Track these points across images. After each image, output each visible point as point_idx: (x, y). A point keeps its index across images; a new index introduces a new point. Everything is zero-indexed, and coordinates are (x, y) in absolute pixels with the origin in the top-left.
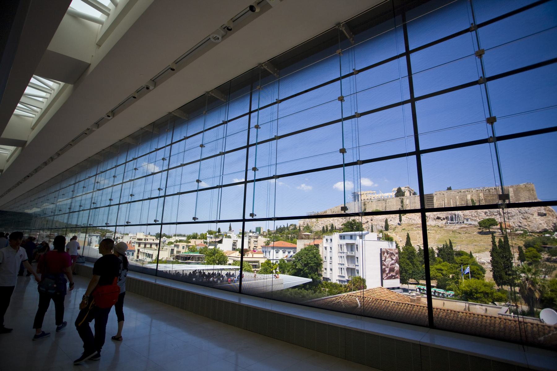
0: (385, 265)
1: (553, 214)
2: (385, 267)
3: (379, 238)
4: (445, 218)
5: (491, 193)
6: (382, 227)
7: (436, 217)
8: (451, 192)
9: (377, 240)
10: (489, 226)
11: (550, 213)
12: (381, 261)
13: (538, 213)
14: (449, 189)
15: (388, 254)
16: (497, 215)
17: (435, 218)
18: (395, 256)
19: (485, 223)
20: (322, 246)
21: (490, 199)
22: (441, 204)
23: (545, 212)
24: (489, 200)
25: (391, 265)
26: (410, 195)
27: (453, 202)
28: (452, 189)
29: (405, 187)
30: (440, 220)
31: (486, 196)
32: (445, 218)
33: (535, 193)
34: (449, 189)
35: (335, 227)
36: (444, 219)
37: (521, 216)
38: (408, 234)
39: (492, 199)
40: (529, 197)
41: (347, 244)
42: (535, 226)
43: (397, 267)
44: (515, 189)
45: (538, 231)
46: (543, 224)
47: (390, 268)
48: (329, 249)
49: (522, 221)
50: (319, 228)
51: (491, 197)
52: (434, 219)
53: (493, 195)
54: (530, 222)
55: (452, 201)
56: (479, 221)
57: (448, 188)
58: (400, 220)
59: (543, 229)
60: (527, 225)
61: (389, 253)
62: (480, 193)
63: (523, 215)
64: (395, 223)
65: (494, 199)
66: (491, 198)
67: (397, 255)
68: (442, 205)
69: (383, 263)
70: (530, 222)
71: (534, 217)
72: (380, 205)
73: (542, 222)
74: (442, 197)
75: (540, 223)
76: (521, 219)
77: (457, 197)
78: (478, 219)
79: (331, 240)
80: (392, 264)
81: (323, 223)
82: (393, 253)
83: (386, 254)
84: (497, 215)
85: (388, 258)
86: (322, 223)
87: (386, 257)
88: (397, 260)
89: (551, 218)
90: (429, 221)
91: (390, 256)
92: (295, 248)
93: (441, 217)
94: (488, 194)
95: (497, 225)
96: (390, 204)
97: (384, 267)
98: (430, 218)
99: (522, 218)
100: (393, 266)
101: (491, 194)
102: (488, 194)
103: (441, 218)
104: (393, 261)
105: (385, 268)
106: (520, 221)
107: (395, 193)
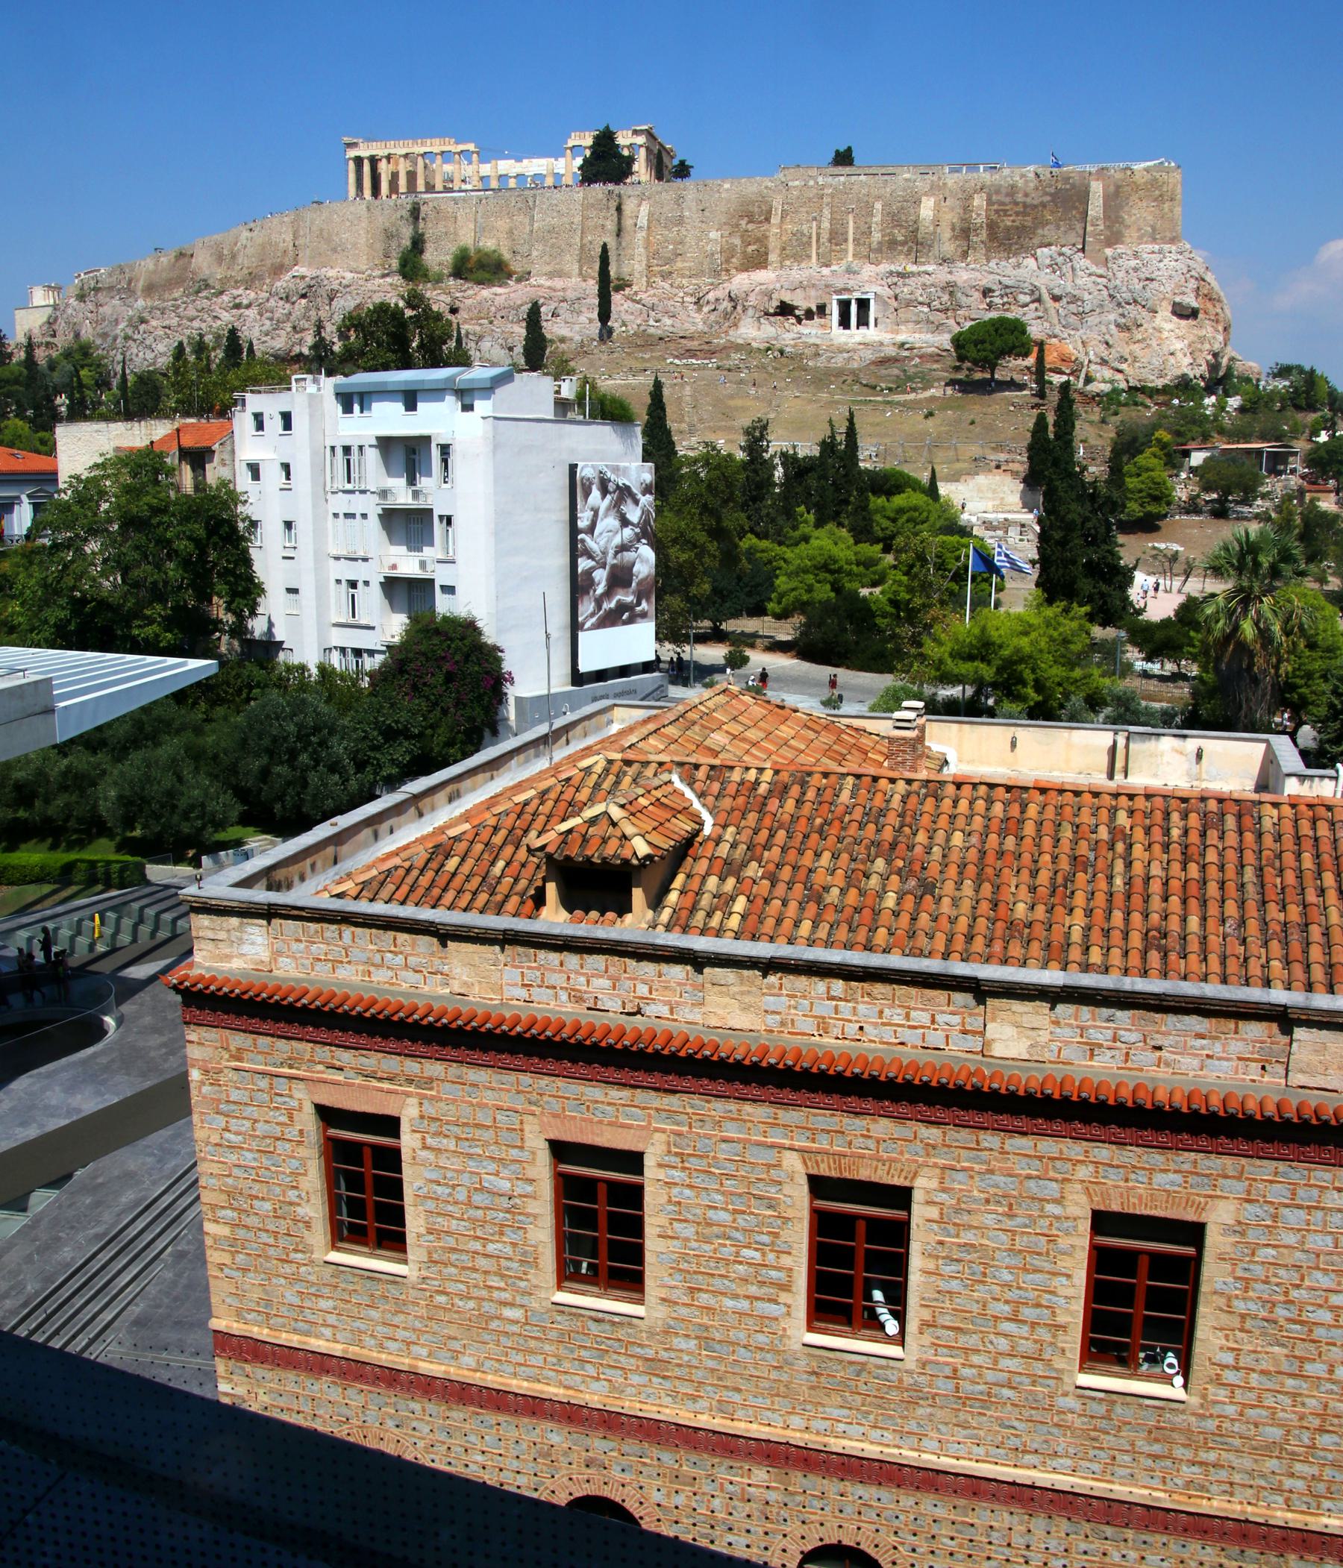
0: (589, 555)
1: (1219, 311)
2: (590, 563)
3: (562, 406)
4: (814, 309)
5: (1020, 198)
6: (511, 349)
7: (775, 303)
8: (854, 178)
9: (552, 417)
10: (998, 358)
11: (1209, 305)
12: (574, 530)
13: (1175, 304)
14: (844, 158)
15: (604, 491)
16: (1026, 305)
17: (772, 311)
18: (636, 502)
19: (983, 342)
20: (226, 456)
21: (1009, 224)
23: (1195, 304)
24: (1008, 229)
25: (616, 553)
27: (856, 228)
29: (636, 132)
30: (793, 320)
31: (997, 211)
32: (814, 309)
33: (1178, 210)
35: (251, 344)
37: (1112, 317)
38: (658, 386)
39: (1017, 228)
40: (1154, 229)
41: (386, 444)
42: (1154, 361)
43: (645, 561)
44: (1112, 189)
45: (1159, 383)
46: (1179, 355)
47: (613, 566)
48: (272, 475)
49: (1117, 337)
50: (150, 356)
51: (1017, 214)
52: (767, 314)
53: (1025, 205)
54: (1139, 341)
55: (851, 224)
56: (957, 329)
57: (837, 153)
58: (605, 314)
59: (1178, 377)
60: (1127, 356)
61: (611, 487)
62: (975, 192)
63: (1121, 310)
64: (577, 327)
65: (1024, 227)
66: (1017, 224)
67: (647, 500)
68: (805, 239)
69: (583, 541)
70: (1139, 341)
71: (1159, 321)
73: (1178, 345)
74: (810, 200)
75: (1172, 348)
76: (1112, 327)
77: (878, 206)
78: (951, 322)
79: (287, 419)
80: (623, 548)
81: (174, 321)
82: (627, 488)
83: (596, 493)
84: (1026, 305)
85: (606, 516)
86: (167, 323)
87: (596, 511)
88: (647, 522)
89: (1208, 330)
90: (742, 323)
91: (617, 505)
92: (52, 477)
93: (795, 303)
94: (1007, 200)
95: (1026, 355)
97: (584, 564)
99: (1118, 326)
100: (629, 556)
101: (1016, 204)
103: (797, 312)
104: (628, 533)
105: (593, 569)
106: (1107, 337)
107: (579, 161)
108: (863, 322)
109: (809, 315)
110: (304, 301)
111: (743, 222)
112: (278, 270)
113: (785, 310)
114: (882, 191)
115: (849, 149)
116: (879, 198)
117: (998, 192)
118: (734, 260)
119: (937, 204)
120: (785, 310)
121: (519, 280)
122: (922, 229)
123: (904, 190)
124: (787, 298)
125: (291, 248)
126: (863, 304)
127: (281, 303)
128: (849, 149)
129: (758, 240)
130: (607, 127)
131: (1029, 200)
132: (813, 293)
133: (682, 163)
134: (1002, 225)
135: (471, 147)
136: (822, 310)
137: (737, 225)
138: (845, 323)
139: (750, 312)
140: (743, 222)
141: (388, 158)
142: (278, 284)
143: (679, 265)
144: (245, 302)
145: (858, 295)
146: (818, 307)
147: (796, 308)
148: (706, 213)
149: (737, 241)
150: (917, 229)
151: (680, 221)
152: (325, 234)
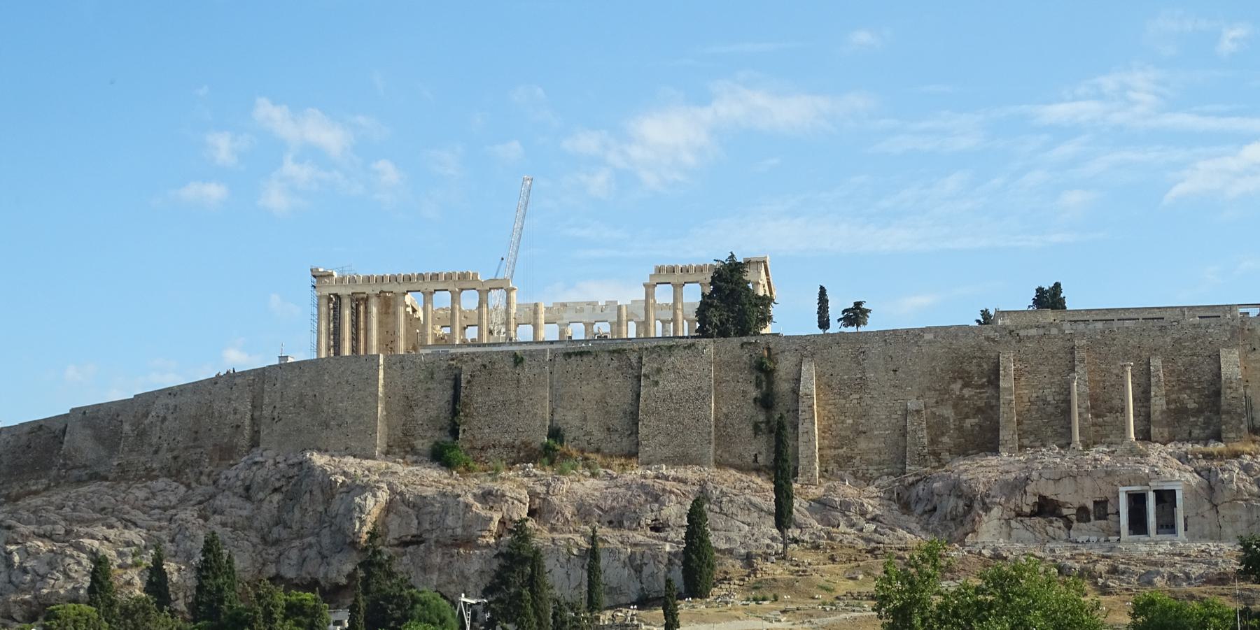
4: (1091, 506)
7: (1032, 499)
17: (1027, 509)
22: (1046, 402)
26: (824, 323)
28: (1069, 306)
32: (1091, 506)
34: (1049, 299)
36: (1083, 513)
52: (1018, 515)
57: (1040, 290)
72: (590, 389)
74: (1053, 355)
77: (1156, 363)
93: (1061, 499)
96: (669, 383)
98: (987, 509)
103: (1065, 512)
108: (1167, 526)
109: (1083, 513)
110: (277, 497)
111: (956, 386)
112: (226, 453)
113: (1046, 508)
115: (1057, 285)
116: (1155, 351)
118: (945, 439)
119: (1244, 357)
120: (1046, 508)
122: (1227, 395)
124: (1049, 491)
125: (247, 422)
127: (236, 501)
128: (1057, 285)
129: (979, 410)
130: (733, 256)
132: (1087, 482)
133: (858, 304)
136: (1102, 509)
137: (947, 391)
138: (1138, 524)
140: (956, 386)
141: (378, 296)
142: (231, 473)
145: (1155, 485)
146: (1095, 502)
147: (1064, 505)
148: (900, 374)
149: (948, 412)
150: (1218, 394)
152: (309, 402)
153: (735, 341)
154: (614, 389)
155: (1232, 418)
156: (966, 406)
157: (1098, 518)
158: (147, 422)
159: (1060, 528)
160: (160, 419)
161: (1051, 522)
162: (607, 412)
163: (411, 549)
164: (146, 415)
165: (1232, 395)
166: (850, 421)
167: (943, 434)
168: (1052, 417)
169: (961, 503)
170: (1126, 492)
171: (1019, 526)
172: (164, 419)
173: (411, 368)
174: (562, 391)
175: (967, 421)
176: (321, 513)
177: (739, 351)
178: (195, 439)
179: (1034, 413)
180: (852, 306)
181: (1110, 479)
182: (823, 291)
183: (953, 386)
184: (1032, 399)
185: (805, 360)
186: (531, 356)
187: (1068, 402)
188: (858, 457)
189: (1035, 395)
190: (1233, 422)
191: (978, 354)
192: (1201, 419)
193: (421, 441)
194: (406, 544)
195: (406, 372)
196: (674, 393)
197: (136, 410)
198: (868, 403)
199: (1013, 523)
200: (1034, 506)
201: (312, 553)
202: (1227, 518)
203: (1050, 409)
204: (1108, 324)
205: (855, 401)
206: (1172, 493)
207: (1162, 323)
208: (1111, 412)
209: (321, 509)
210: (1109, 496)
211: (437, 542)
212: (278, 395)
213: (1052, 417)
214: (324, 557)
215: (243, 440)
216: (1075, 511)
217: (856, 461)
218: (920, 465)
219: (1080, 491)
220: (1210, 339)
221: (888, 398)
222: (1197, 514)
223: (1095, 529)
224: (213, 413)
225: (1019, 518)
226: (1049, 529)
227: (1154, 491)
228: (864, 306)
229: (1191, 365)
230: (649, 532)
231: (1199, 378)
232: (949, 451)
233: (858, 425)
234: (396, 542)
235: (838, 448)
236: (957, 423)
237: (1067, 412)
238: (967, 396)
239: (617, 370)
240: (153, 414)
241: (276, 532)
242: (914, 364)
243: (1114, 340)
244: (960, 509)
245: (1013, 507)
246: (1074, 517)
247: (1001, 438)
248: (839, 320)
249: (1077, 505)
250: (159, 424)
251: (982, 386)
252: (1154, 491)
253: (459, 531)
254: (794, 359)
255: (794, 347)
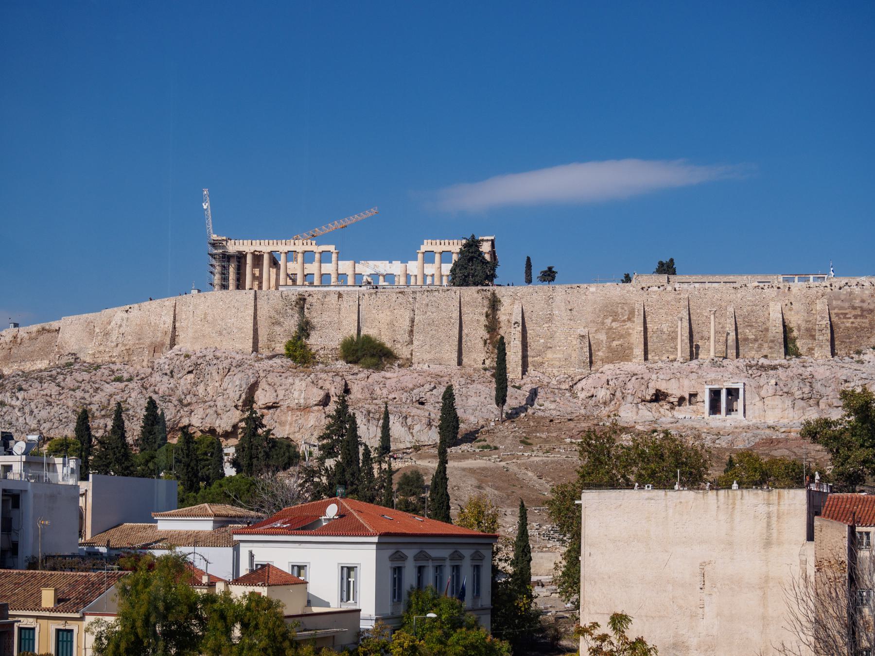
5: (857, 303)
8: (707, 285)
17: (648, 398)
21: (848, 325)
22: (662, 332)
24: (848, 329)
30: (668, 406)
31: (837, 315)
32: (687, 397)
36: (681, 400)
39: (856, 328)
51: (856, 317)
52: (643, 401)
57: (661, 264)
74: (668, 303)
93: (670, 392)
94: (846, 305)
101: (854, 308)
102: (846, 305)
103: (672, 399)
111: (608, 321)
113: (659, 397)
114: (733, 297)
115: (672, 260)
117: (837, 298)
118: (600, 354)
120: (659, 397)
121: (400, 366)
123: (754, 296)
124: (663, 387)
126: (733, 393)
127: (166, 378)
128: (672, 260)
130: (473, 236)
131: (865, 305)
132: (686, 382)
133: (550, 269)
134: (842, 326)
135: (332, 248)
137: (603, 323)
138: (715, 408)
139: (629, 398)
140: (608, 321)
143: (550, 355)
144: (126, 376)
146: (691, 395)
148: (574, 312)
149: (602, 337)
150: (767, 330)
151: (550, 319)
152: (209, 318)
153: (474, 289)
154: (398, 317)
155: (775, 345)
156: (614, 333)
157: (690, 403)
158: (109, 327)
159: (668, 410)
160: (118, 325)
161: (661, 406)
162: (394, 330)
163: (271, 411)
164: (109, 323)
165: (776, 331)
166: (542, 341)
167: (599, 350)
168: (666, 342)
169: (609, 393)
170: (710, 389)
171: (644, 408)
172: (121, 326)
173: (274, 299)
174: (366, 317)
175: (614, 342)
176: (217, 387)
177: (476, 295)
178: (139, 339)
179: (655, 338)
180: (546, 269)
181: (700, 380)
182: (529, 259)
183: (606, 321)
184: (654, 330)
185: (517, 302)
186: (348, 294)
187: (676, 332)
188: (547, 363)
189: (656, 328)
190: (776, 347)
191: (623, 301)
192: (756, 345)
193: (279, 345)
194: (269, 408)
195: (270, 301)
196: (435, 320)
197: (103, 319)
198: (554, 329)
199: (640, 406)
200: (652, 396)
201: (211, 411)
202: (770, 406)
203: (665, 337)
204: (703, 285)
205: (546, 328)
206: (737, 390)
207: (735, 285)
208: (701, 339)
209: (217, 384)
210: (699, 391)
211: (288, 407)
212: (192, 313)
213: (666, 342)
214: (218, 415)
215: (168, 341)
216: (677, 400)
217: (546, 365)
218: (584, 369)
219: (681, 388)
220: (764, 296)
221: (566, 327)
222: (751, 403)
223: (689, 410)
224: (150, 323)
225: (643, 403)
226: (661, 410)
227: (726, 389)
228: (553, 270)
229: (752, 312)
230: (418, 405)
231: (756, 320)
232: (602, 360)
233: (547, 343)
234: (264, 406)
235: (535, 357)
236: (608, 344)
237: (674, 339)
238: (614, 327)
239: (401, 304)
240: (114, 322)
241: (189, 399)
242: (583, 306)
243: (705, 294)
244: (608, 396)
245: (640, 396)
246: (677, 403)
247: (634, 353)
248: (538, 277)
249: (679, 396)
250: (117, 329)
251: (624, 321)
252: (726, 389)
253: (302, 401)
254: (510, 301)
255: (510, 293)
